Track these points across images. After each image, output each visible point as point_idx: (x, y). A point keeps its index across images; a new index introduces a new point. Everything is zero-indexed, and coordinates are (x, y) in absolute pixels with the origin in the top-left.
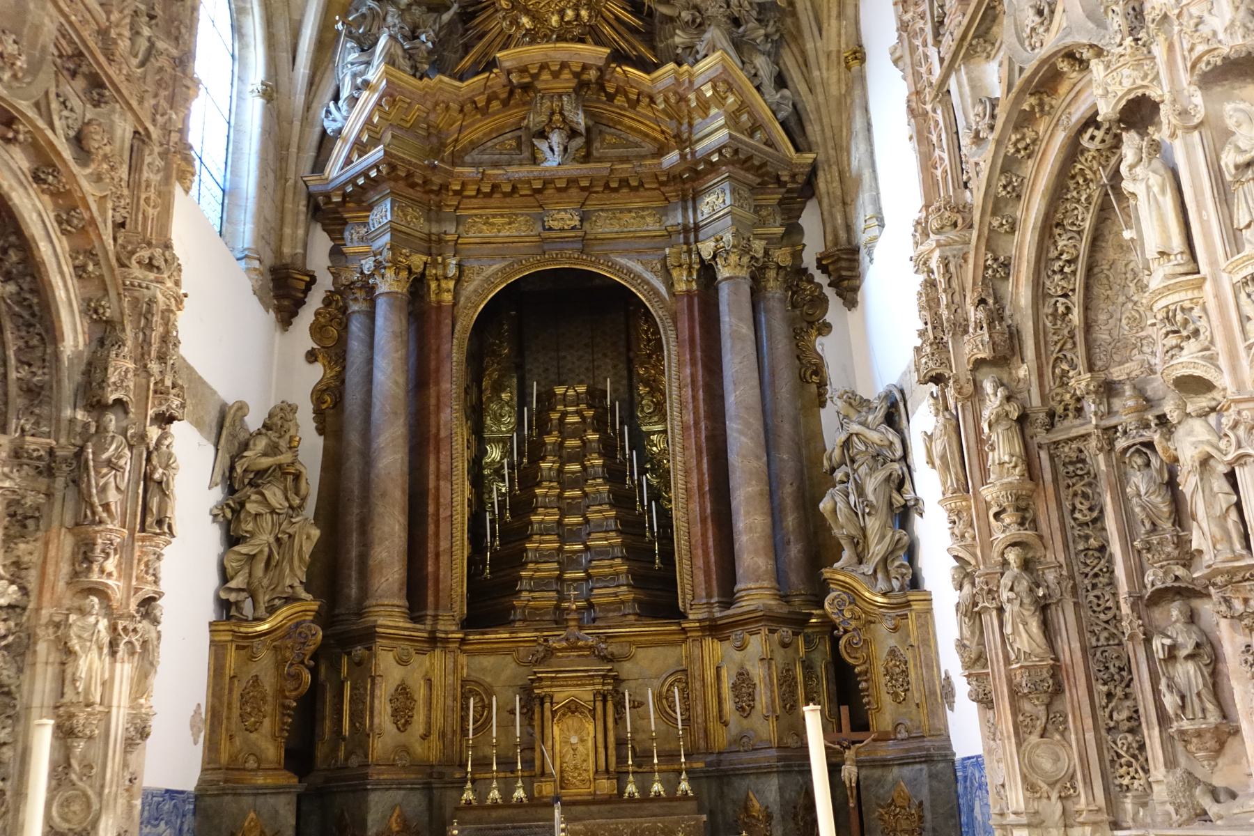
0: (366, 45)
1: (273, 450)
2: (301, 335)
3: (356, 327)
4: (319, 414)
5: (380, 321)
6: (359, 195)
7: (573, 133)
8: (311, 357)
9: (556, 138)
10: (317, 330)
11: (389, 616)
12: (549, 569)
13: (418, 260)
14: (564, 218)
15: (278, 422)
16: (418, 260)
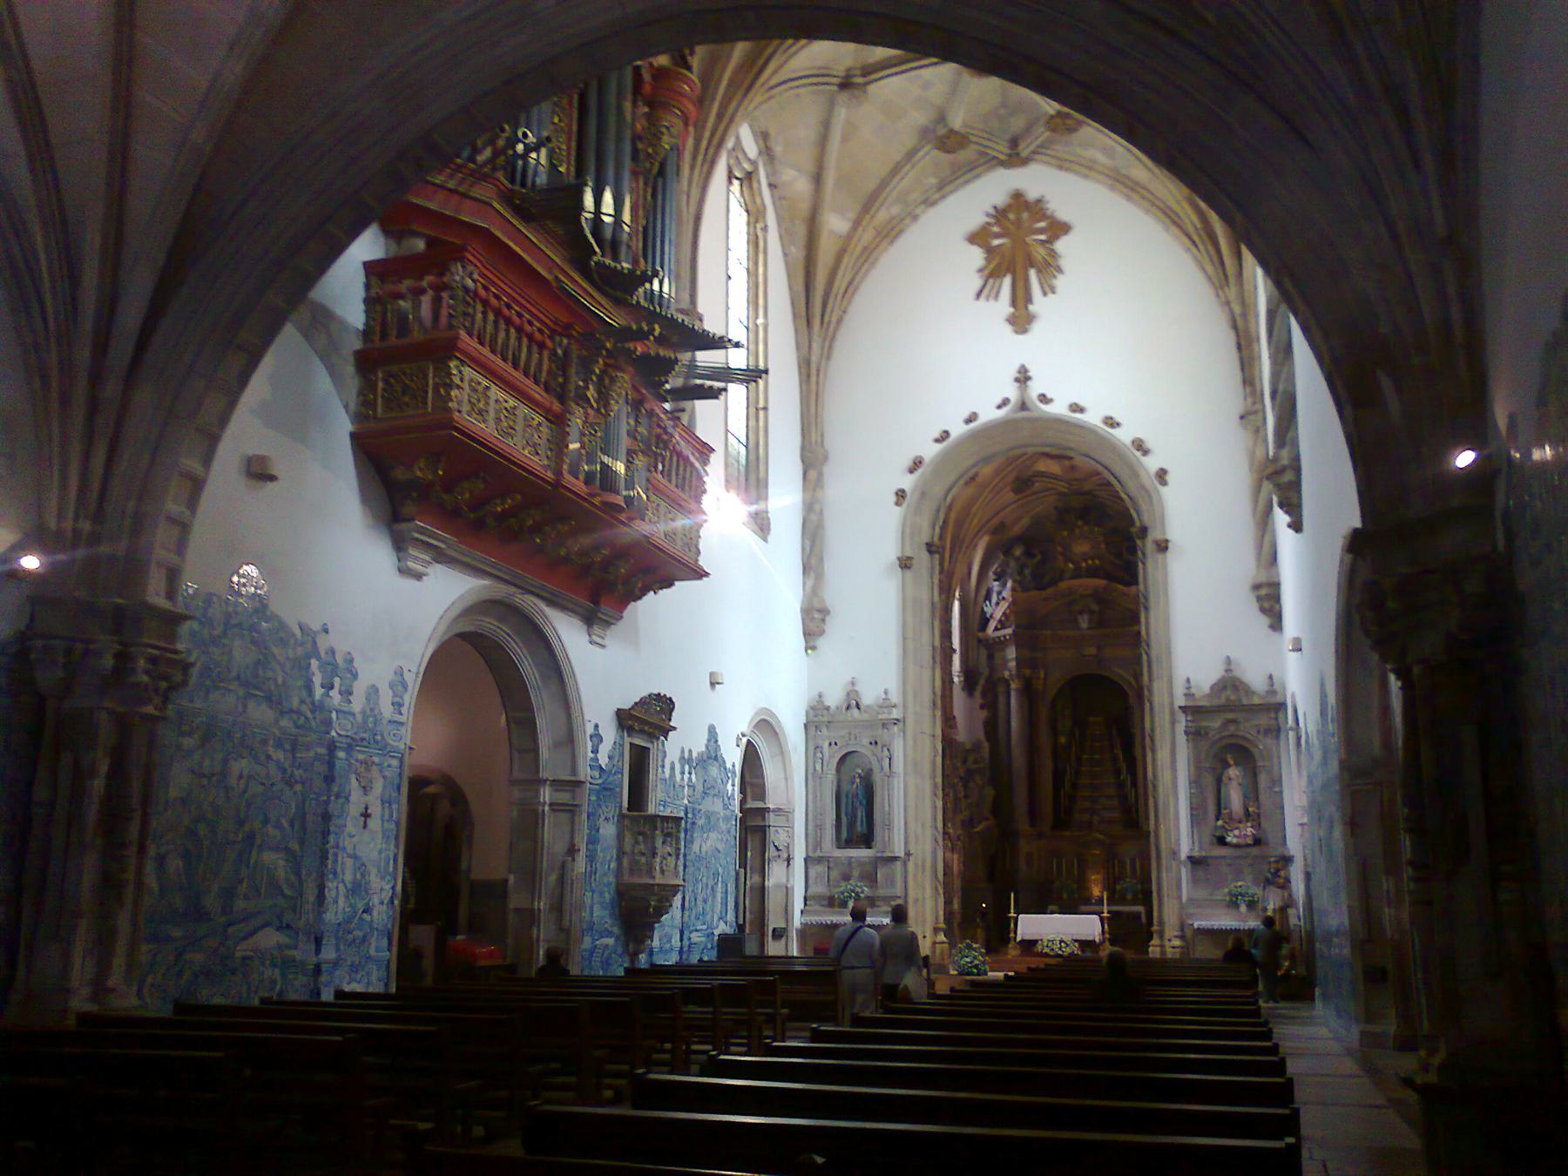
0: (999, 577)
1: (975, 762)
2: (978, 700)
3: (1002, 699)
4: (987, 733)
5: (1013, 701)
6: (1001, 644)
7: (1091, 612)
8: (982, 707)
9: (1086, 617)
10: (984, 695)
11: (1023, 826)
12: (1087, 804)
13: (1027, 672)
14: (1092, 651)
15: (976, 747)
16: (1027, 672)
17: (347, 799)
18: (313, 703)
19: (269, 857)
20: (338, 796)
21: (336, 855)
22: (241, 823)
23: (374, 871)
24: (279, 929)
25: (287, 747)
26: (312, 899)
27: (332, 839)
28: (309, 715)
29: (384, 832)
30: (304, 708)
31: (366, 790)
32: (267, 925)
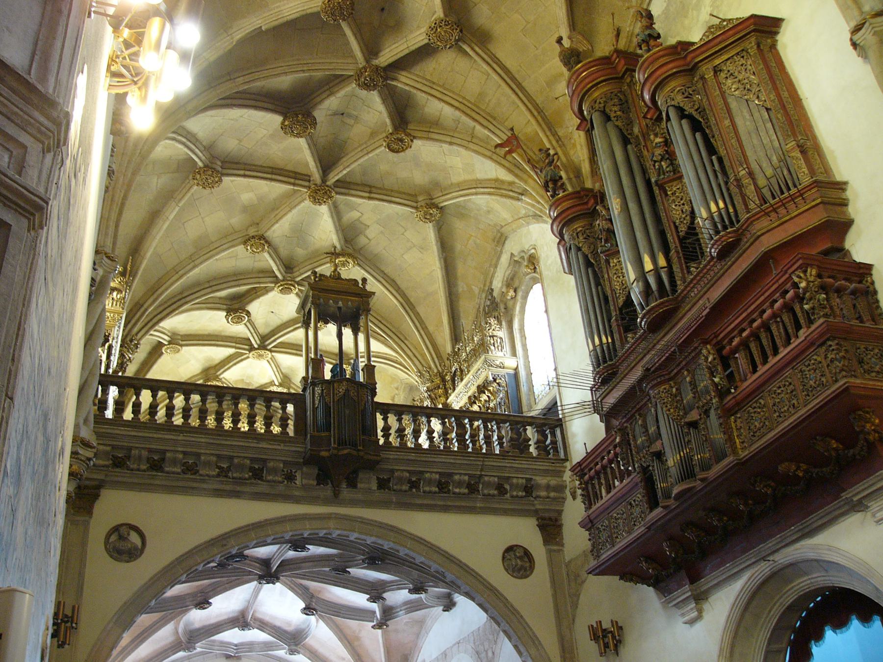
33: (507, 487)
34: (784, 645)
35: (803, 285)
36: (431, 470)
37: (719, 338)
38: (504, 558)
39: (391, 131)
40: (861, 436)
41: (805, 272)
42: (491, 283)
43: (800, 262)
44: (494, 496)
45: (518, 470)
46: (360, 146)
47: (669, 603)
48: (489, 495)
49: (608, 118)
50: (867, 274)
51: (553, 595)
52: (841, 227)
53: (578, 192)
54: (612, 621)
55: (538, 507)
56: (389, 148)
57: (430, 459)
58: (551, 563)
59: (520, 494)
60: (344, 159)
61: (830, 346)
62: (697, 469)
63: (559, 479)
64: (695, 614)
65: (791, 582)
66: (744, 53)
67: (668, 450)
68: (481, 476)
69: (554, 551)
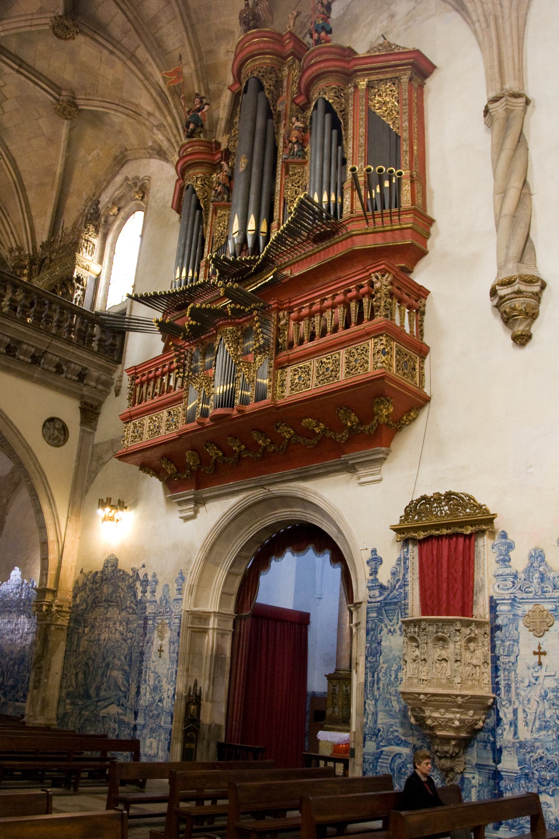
17: (152, 643)
18: (137, 601)
19: (115, 673)
20: (148, 643)
21: (146, 671)
22: (104, 660)
23: (165, 680)
24: (118, 705)
25: (125, 624)
26: (133, 693)
27: (144, 663)
28: (135, 607)
29: (170, 658)
30: (132, 605)
31: (162, 638)
32: (113, 703)
33: (65, 368)
34: (252, 554)
35: (377, 285)
36: (5, 333)
37: (292, 304)
38: (44, 426)
39: (60, 14)
40: (376, 418)
41: (383, 276)
42: (100, 195)
43: (383, 266)
44: (51, 372)
45: (78, 357)
46: (26, 15)
47: (173, 499)
48: (48, 370)
49: (261, 88)
50: (424, 297)
51: (75, 467)
52: (419, 253)
53: (211, 143)
54: (119, 500)
55: (86, 393)
56: (53, 30)
57: (7, 324)
58: (82, 440)
59: (74, 377)
60: (6, 21)
61: (381, 340)
62: (237, 401)
63: (109, 376)
64: (192, 513)
65: (276, 509)
66: (397, 81)
67: (218, 379)
68: (46, 352)
69: (87, 432)
